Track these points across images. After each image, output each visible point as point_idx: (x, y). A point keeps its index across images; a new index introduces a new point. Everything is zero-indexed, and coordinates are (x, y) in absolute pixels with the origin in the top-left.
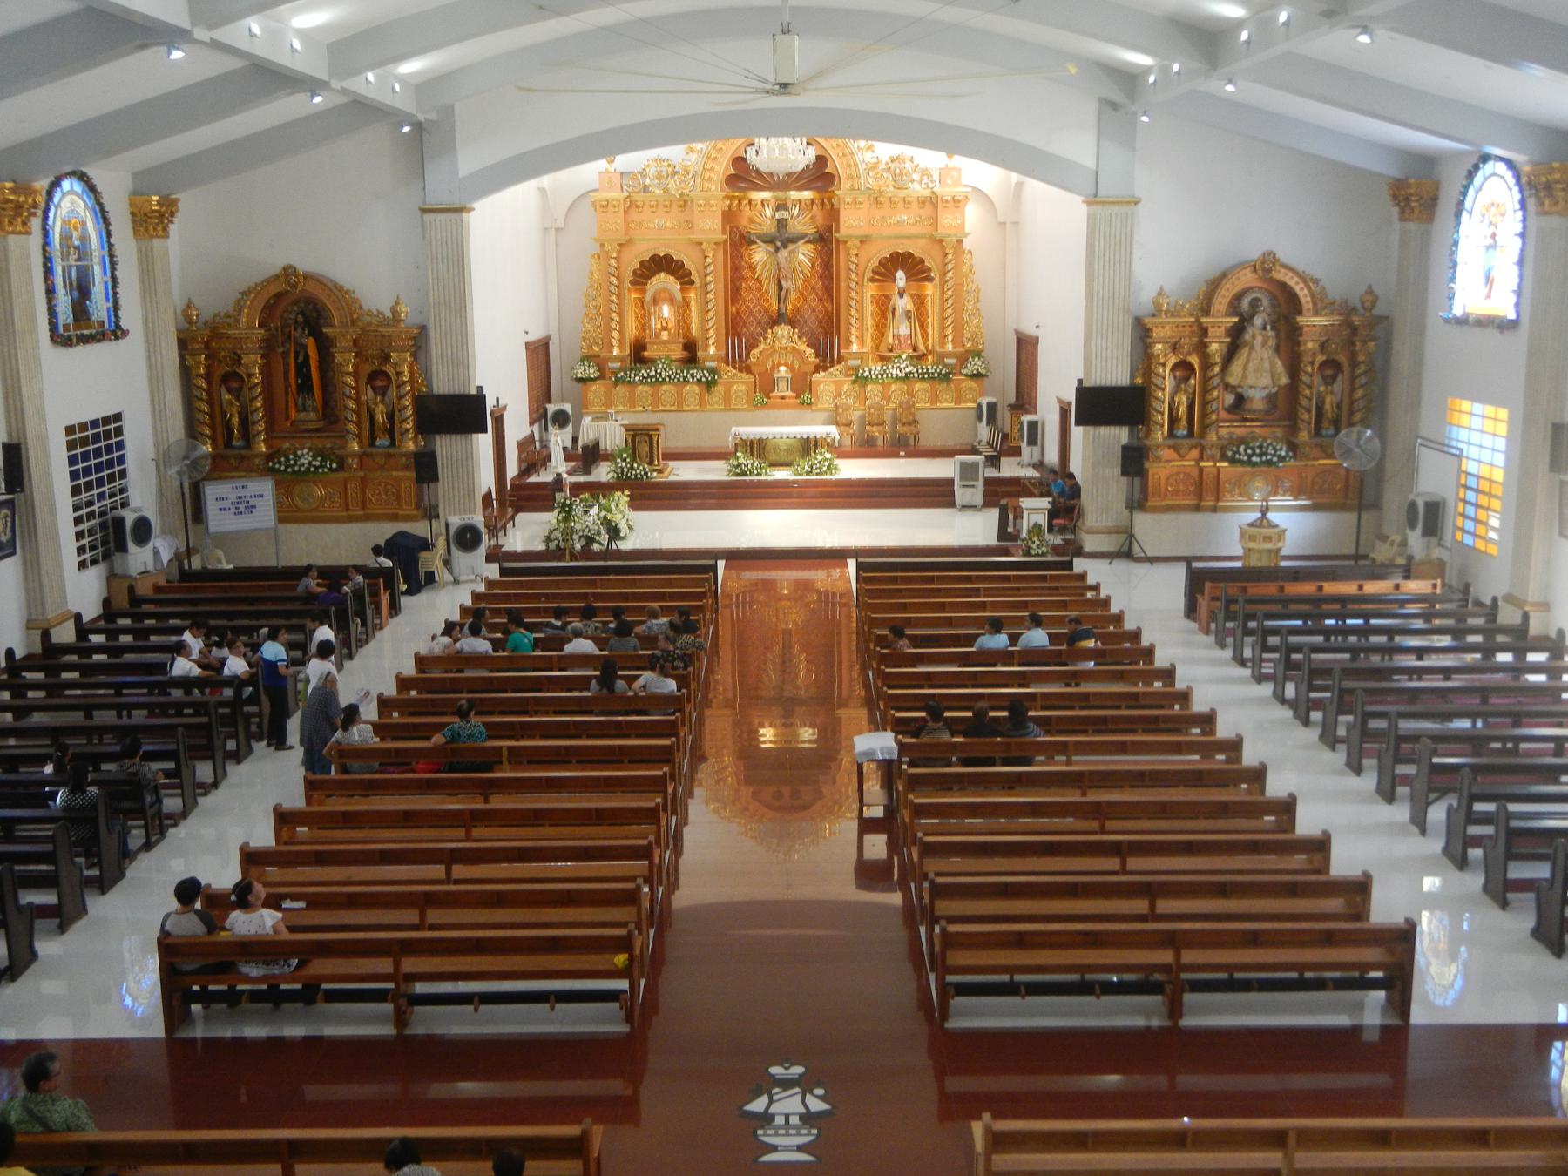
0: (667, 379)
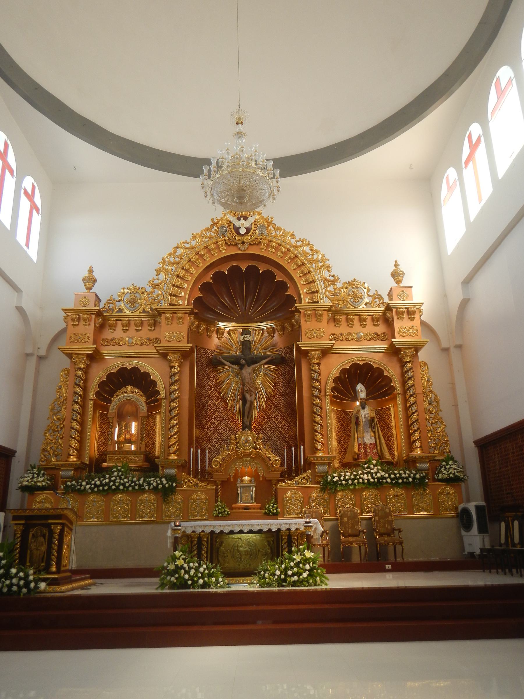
0: (121, 487)
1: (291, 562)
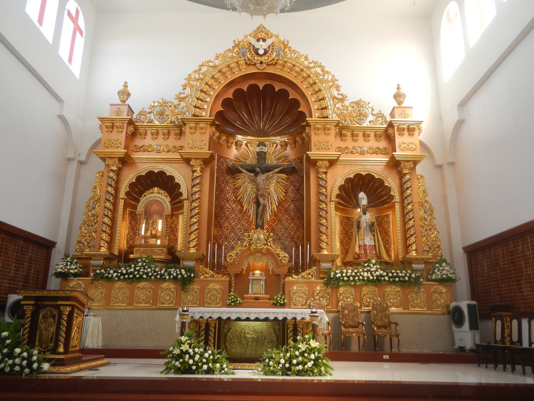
0: (145, 276)
1: (296, 351)
